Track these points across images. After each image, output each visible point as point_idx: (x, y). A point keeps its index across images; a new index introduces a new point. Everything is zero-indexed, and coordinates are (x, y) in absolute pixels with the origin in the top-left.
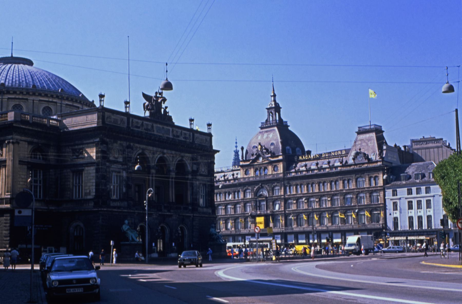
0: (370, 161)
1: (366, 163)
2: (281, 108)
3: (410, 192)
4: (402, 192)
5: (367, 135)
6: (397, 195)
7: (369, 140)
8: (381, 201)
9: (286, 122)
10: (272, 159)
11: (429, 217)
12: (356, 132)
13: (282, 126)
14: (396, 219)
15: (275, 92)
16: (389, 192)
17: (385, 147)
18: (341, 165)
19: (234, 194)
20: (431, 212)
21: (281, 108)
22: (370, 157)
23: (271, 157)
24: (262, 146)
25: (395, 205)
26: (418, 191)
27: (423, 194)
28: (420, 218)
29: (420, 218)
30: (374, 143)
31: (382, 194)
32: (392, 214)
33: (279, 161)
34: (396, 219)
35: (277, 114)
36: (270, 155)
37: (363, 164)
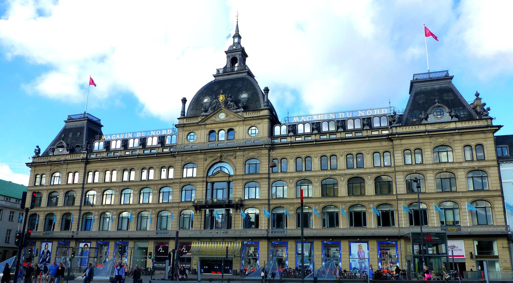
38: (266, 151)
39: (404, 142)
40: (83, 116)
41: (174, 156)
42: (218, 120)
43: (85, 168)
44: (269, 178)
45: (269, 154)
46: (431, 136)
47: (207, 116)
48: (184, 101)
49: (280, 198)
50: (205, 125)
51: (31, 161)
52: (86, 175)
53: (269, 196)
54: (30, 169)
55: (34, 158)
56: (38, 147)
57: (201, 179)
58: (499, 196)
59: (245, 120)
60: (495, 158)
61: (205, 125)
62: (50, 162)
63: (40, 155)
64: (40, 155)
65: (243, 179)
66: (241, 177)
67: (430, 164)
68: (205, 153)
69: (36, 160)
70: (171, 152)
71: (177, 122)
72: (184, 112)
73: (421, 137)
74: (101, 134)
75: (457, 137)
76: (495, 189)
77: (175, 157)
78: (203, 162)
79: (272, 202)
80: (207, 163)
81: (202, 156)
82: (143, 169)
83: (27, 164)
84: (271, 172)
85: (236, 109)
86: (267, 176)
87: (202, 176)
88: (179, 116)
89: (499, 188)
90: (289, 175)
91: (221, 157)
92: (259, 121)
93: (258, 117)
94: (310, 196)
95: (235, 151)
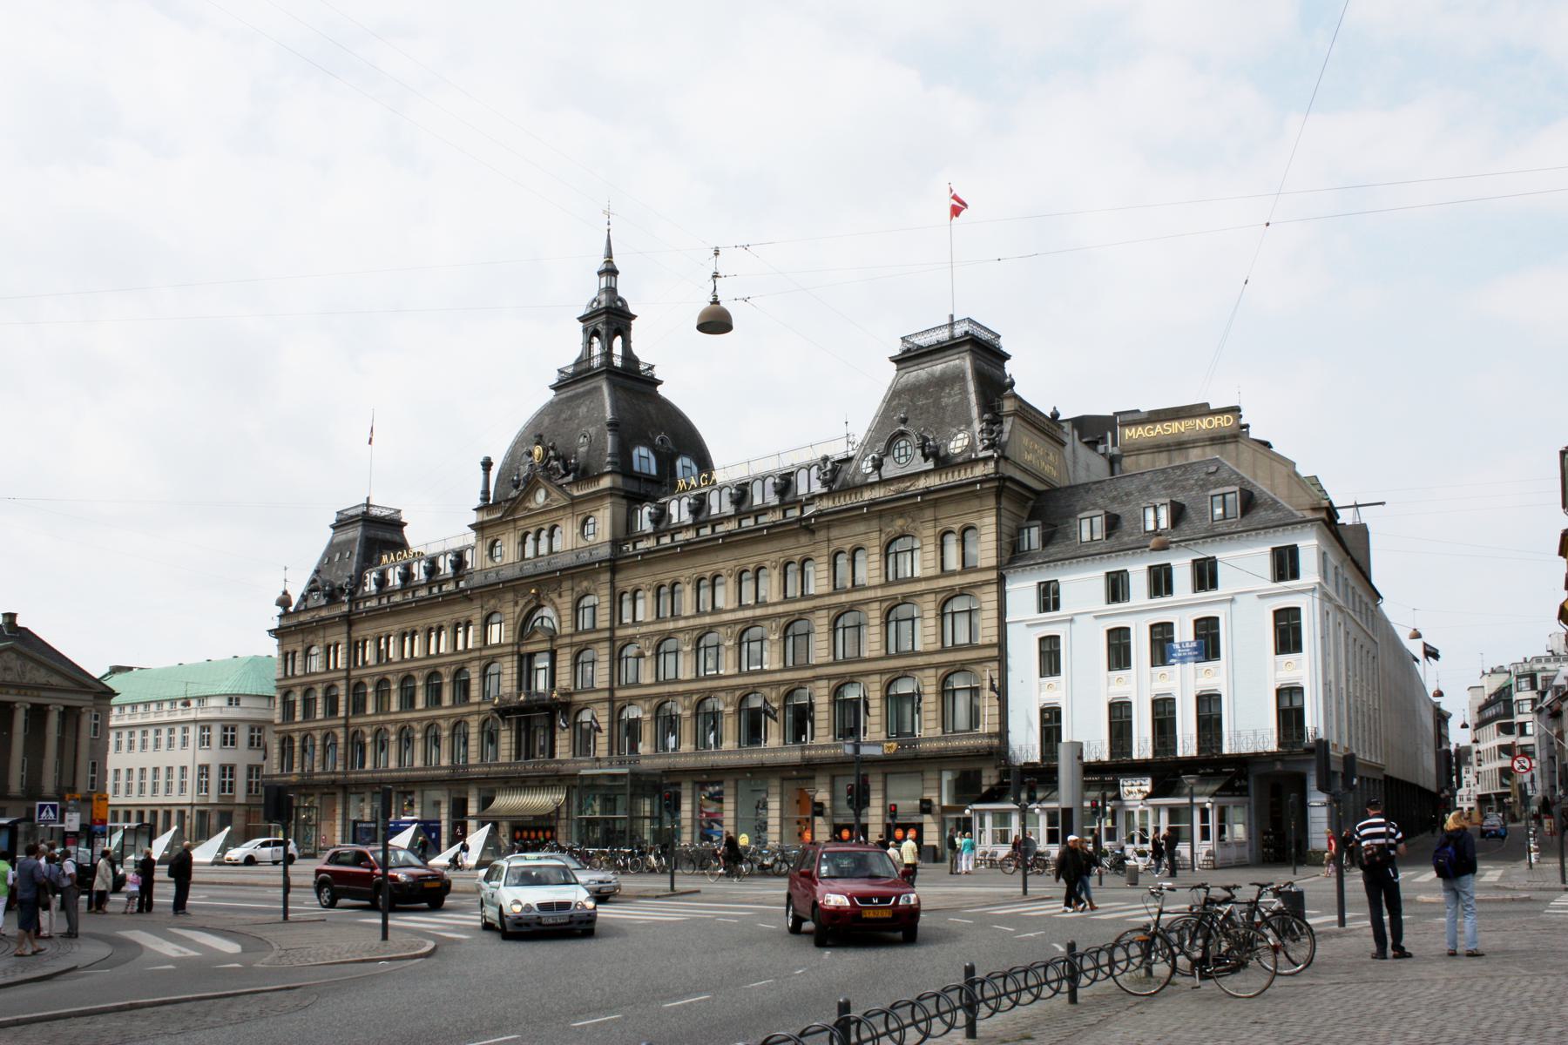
0: (944, 463)
1: (926, 473)
4: (1082, 586)
5: (938, 367)
6: (1057, 607)
7: (942, 382)
8: (987, 633)
9: (651, 367)
10: (576, 493)
13: (634, 382)
15: (616, 260)
17: (1008, 406)
18: (825, 490)
19: (456, 633)
22: (942, 453)
23: (576, 482)
24: (546, 451)
26: (1161, 582)
30: (965, 391)
31: (989, 598)
33: (598, 496)
35: (618, 343)
36: (570, 478)
37: (917, 475)
38: (606, 577)
39: (834, 533)
40: (360, 511)
41: (469, 599)
42: (533, 505)
44: (612, 640)
45: (612, 582)
47: (514, 499)
48: (487, 465)
49: (712, 678)
50: (515, 520)
51: (275, 624)
52: (354, 647)
53: (612, 681)
54: (276, 641)
57: (509, 649)
59: (574, 502)
60: (993, 562)
62: (302, 624)
63: (291, 609)
64: (291, 609)
66: (567, 640)
67: (874, 587)
68: (514, 589)
69: (285, 622)
70: (463, 590)
71: (474, 518)
73: (862, 518)
74: (402, 545)
75: (929, 514)
76: (987, 641)
78: (511, 611)
79: (619, 694)
80: (518, 609)
81: (510, 596)
82: (458, 625)
86: (607, 634)
87: (510, 640)
89: (995, 640)
90: (644, 629)
91: (537, 595)
92: (597, 504)
94: (681, 677)
95: (559, 581)
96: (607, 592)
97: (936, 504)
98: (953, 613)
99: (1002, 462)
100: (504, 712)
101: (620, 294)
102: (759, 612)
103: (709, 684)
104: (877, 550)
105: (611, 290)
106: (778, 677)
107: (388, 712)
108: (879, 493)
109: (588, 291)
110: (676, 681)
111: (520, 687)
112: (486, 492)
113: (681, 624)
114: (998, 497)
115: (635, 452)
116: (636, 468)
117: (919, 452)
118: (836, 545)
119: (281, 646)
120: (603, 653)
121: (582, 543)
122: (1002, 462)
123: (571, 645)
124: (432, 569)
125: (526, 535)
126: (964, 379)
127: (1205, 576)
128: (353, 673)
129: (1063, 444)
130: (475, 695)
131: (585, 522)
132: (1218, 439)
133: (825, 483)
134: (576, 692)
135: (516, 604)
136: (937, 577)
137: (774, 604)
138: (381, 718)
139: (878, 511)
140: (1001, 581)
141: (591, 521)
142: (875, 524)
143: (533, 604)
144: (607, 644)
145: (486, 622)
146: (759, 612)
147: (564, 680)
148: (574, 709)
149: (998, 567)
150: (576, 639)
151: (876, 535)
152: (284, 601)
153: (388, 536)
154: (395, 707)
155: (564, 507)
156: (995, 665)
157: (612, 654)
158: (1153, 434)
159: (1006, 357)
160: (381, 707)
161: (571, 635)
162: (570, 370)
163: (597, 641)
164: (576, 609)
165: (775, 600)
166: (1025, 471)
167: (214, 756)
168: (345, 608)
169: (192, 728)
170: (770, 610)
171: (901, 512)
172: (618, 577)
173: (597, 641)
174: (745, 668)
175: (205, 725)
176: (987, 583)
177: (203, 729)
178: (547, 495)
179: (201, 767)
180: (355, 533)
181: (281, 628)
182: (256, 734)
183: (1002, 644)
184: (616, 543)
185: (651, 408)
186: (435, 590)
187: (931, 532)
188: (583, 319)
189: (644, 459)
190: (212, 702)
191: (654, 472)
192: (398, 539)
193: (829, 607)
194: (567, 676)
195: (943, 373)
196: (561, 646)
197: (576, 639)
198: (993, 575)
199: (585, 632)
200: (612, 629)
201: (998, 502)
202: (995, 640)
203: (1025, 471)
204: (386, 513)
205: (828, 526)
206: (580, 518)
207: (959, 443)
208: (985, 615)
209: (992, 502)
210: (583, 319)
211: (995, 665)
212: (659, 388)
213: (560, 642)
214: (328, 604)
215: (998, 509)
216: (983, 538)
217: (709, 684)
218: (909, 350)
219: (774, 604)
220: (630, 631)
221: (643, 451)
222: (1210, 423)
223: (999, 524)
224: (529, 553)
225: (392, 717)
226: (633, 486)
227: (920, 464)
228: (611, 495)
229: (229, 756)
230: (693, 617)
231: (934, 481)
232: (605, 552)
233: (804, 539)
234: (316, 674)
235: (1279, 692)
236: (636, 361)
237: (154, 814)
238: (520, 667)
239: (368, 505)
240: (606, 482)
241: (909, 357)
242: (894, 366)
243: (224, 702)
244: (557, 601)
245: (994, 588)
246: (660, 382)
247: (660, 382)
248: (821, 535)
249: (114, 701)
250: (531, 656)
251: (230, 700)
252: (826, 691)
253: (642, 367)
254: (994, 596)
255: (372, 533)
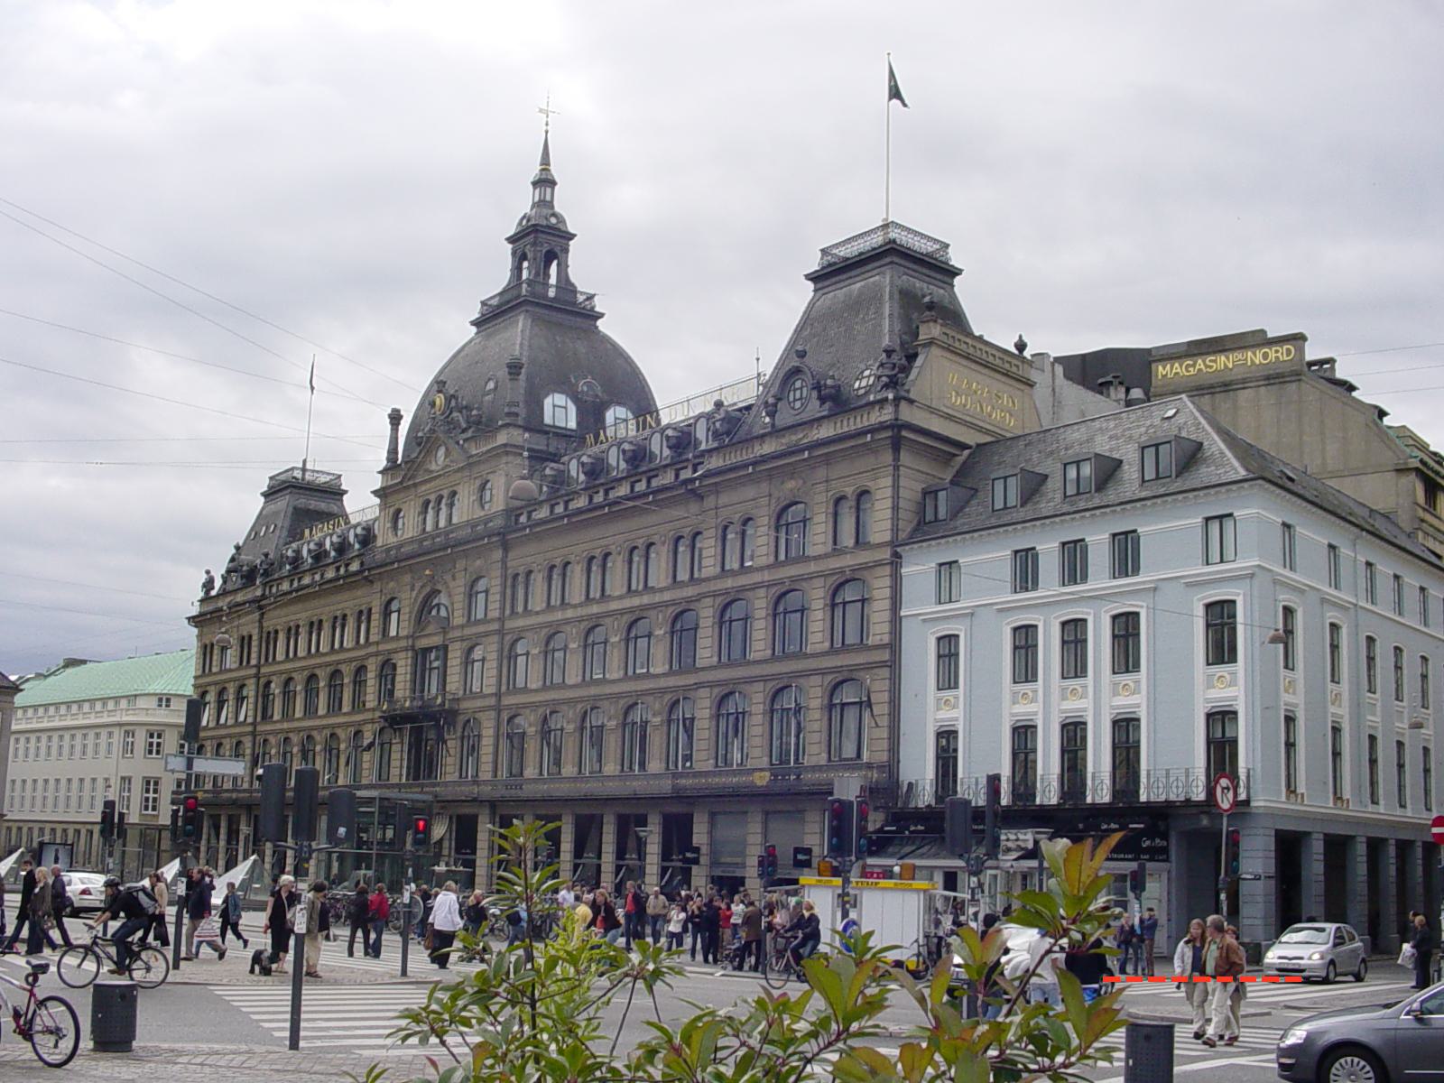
2: (572, 236)
3: (1025, 570)
9: (590, 297)
11: (1125, 728)
12: (809, 277)
14: (946, 738)
16: (919, 569)
18: (716, 445)
20: (1133, 696)
21: (572, 236)
24: (449, 399)
25: (948, 649)
26: (1074, 563)
27: (1100, 577)
28: (1073, 734)
29: (1073, 734)
32: (927, 710)
34: (946, 738)
36: (469, 433)
38: (498, 554)
39: (724, 499)
42: (433, 467)
43: (260, 622)
44: (501, 632)
45: (504, 561)
46: (770, 475)
48: (395, 418)
50: (415, 485)
51: (195, 611)
54: (195, 631)
55: (202, 601)
56: (208, 572)
57: (403, 643)
58: (882, 664)
61: (415, 485)
63: (213, 593)
64: (213, 593)
65: (462, 639)
72: (397, 453)
75: (821, 473)
77: (372, 582)
80: (414, 594)
81: (407, 578)
83: (189, 619)
84: (508, 612)
85: (464, 431)
87: (403, 633)
88: (383, 463)
89: (886, 639)
93: (488, 451)
96: (498, 573)
97: (828, 460)
98: (845, 604)
99: (903, 404)
100: (394, 721)
101: (557, 209)
102: (646, 599)
103: (594, 691)
104: (765, 520)
105: (544, 204)
106: (662, 683)
107: (293, 720)
108: (768, 448)
109: (522, 203)
110: (563, 686)
111: (414, 691)
112: (393, 451)
113: (570, 613)
114: (896, 445)
115: (548, 402)
116: (548, 420)
117: (815, 394)
118: (724, 513)
119: (200, 636)
120: (487, 651)
121: (479, 513)
122: (903, 404)
123: (462, 639)
124: (342, 548)
125: (427, 503)
126: (881, 299)
127: (1126, 554)
128: (263, 670)
129: (1031, 385)
130: (371, 699)
131: (482, 488)
132: (1275, 378)
133: (716, 435)
134: (464, 698)
135: (412, 590)
136: (826, 556)
137: (661, 590)
138: (286, 726)
139: (766, 469)
140: (896, 561)
141: (489, 486)
142: (764, 487)
143: (428, 589)
144: (496, 638)
145: (386, 614)
146: (646, 599)
147: (454, 683)
148: (461, 719)
149: (894, 544)
150: (468, 631)
151: (764, 501)
152: (209, 585)
153: (323, 506)
154: (298, 714)
155: (459, 470)
156: (885, 672)
157: (501, 650)
158: (1192, 371)
159: (955, 273)
160: (287, 715)
161: (462, 627)
162: (495, 302)
163: (487, 634)
164: (471, 595)
165: (663, 584)
166: (949, 417)
167: (141, 766)
168: (259, 593)
169: (116, 731)
170: (657, 598)
171: (791, 472)
172: (511, 555)
173: (487, 634)
174: (630, 672)
175: (129, 730)
176: (878, 564)
177: (127, 732)
178: (448, 454)
179: (123, 779)
180: (283, 503)
181: (201, 615)
182: (155, 740)
183: (894, 646)
184: (511, 513)
185: (581, 348)
186: (342, 571)
187: (821, 498)
188: (511, 240)
189: (560, 411)
190: (141, 703)
191: (572, 424)
192: (335, 509)
193: (714, 595)
194: (456, 678)
195: (861, 293)
196: (453, 640)
197: (468, 631)
198: (886, 554)
199: (478, 622)
200: (501, 620)
201: (896, 459)
202: (886, 639)
203: (949, 417)
204: (323, 479)
205: (716, 489)
206: (478, 483)
207: (864, 383)
208: (877, 606)
209: (888, 457)
210: (511, 240)
211: (885, 672)
212: (599, 323)
213: (450, 635)
214: (244, 587)
215: (896, 468)
216: (878, 505)
217: (594, 691)
218: (830, 265)
219: (661, 590)
220: (520, 623)
221: (560, 399)
222: (1265, 356)
223: (896, 487)
224: (429, 527)
225: (296, 724)
226: (540, 443)
227: (815, 408)
228: (507, 453)
229: (153, 768)
230: (581, 605)
231: (826, 431)
232: (498, 523)
233: (694, 507)
234: (231, 670)
235: (1210, 716)
236: (574, 291)
237: (78, 832)
238: (415, 665)
239: (304, 470)
240: (502, 438)
241: (830, 274)
242: (811, 285)
243: (154, 702)
244: (452, 584)
245: (887, 570)
246: (601, 315)
247: (601, 315)
248: (710, 502)
249: (19, 699)
250: (427, 650)
251: (160, 700)
252: (707, 703)
253: (581, 298)
254: (887, 582)
255: (302, 502)
